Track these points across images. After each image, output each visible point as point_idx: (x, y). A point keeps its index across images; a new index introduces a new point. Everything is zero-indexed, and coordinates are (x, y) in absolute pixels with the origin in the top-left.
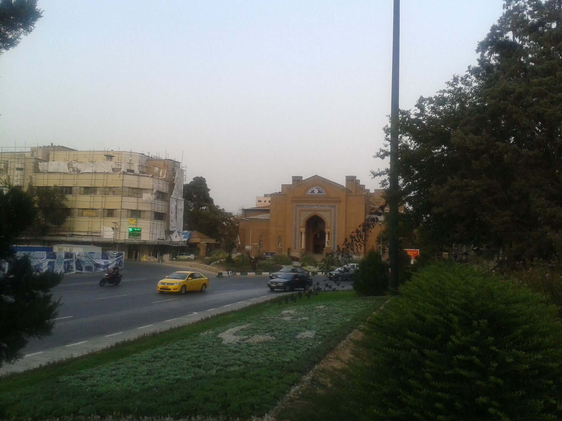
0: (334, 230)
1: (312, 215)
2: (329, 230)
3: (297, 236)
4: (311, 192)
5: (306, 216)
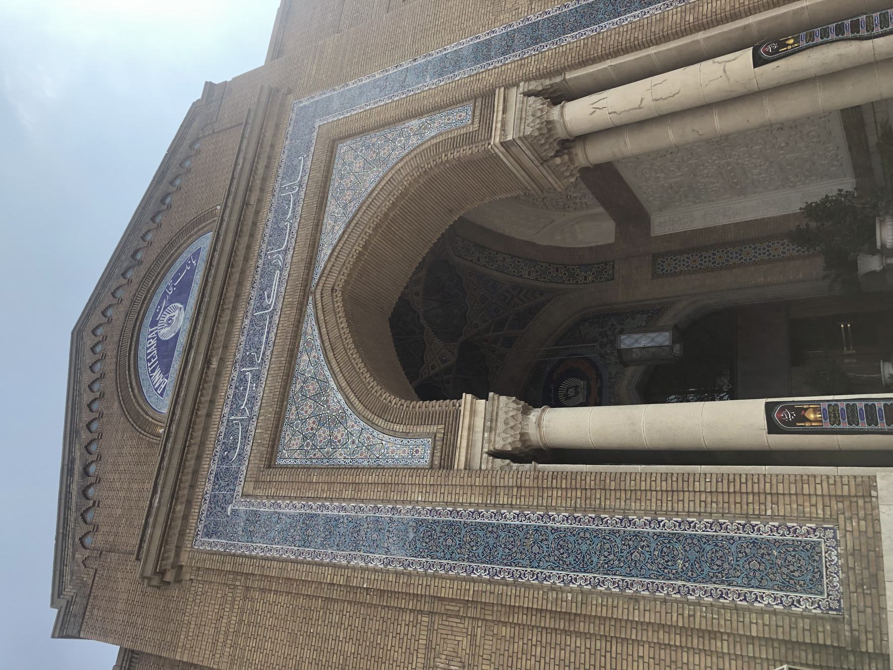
4: (166, 372)
5: (336, 400)
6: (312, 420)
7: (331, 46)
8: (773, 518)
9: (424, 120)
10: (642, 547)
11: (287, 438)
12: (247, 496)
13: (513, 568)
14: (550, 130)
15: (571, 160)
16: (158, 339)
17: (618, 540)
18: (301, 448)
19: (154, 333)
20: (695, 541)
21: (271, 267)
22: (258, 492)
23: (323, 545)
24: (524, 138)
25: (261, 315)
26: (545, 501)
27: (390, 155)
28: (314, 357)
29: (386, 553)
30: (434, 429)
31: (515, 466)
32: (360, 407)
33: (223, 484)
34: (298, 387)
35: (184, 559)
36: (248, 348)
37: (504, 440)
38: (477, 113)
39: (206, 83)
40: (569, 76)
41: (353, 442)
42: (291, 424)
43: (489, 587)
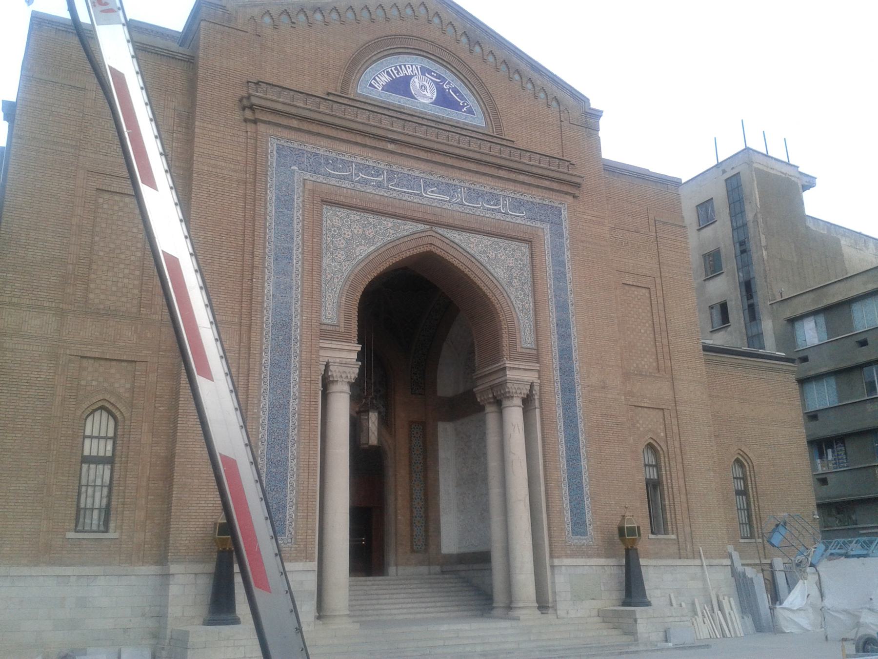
0: (567, 371)
1: (407, 251)
2: (532, 377)
3: (293, 405)
5: (363, 251)
6: (350, 233)
7: (602, 231)
8: (296, 515)
9: (531, 312)
10: (281, 450)
11: (339, 214)
12: (304, 184)
13: (268, 378)
14: (508, 397)
15: (490, 403)
16: (411, 77)
17: (284, 438)
18: (333, 226)
19: (416, 72)
20: (285, 478)
21: (452, 192)
22: (307, 192)
23: (277, 246)
24: (505, 382)
25: (421, 185)
26: (303, 397)
27: (513, 287)
28: (390, 233)
29: (273, 295)
30: (342, 325)
31: (320, 377)
32: (356, 271)
33: (311, 161)
34: (371, 220)
35: (262, 128)
36: (399, 176)
37: (335, 371)
38: (528, 351)
39: (602, 112)
40: (537, 410)
41: (335, 267)
42: (348, 216)
43: (258, 363)
